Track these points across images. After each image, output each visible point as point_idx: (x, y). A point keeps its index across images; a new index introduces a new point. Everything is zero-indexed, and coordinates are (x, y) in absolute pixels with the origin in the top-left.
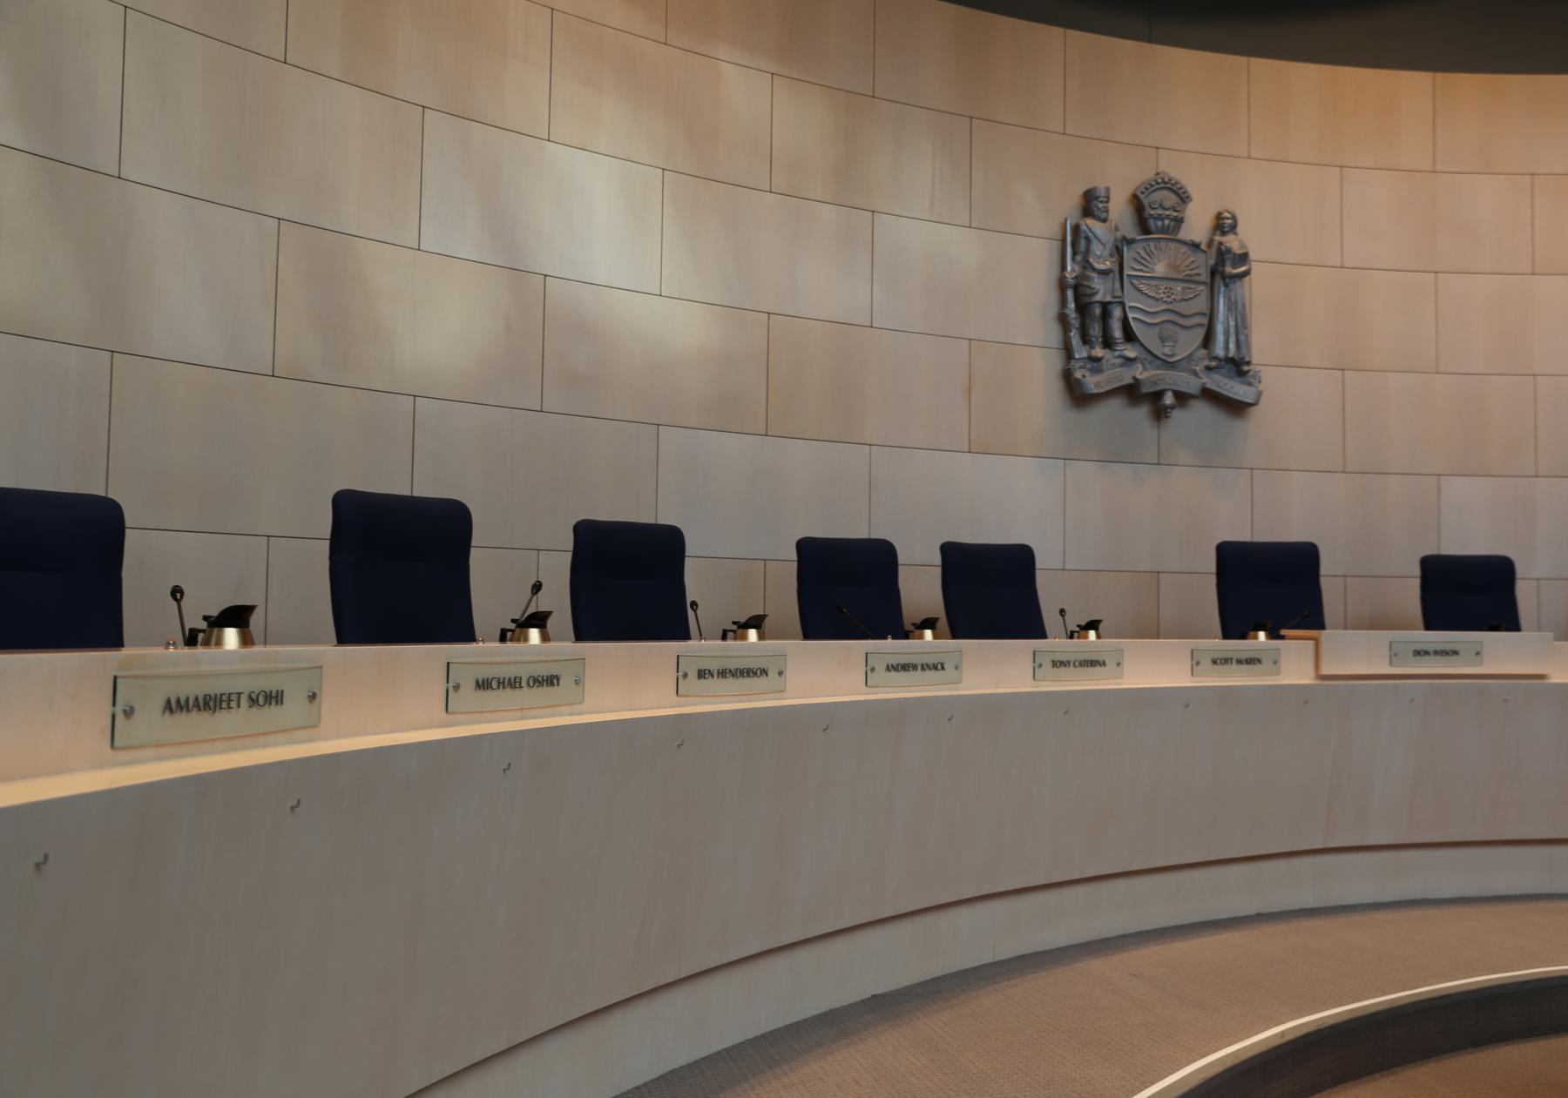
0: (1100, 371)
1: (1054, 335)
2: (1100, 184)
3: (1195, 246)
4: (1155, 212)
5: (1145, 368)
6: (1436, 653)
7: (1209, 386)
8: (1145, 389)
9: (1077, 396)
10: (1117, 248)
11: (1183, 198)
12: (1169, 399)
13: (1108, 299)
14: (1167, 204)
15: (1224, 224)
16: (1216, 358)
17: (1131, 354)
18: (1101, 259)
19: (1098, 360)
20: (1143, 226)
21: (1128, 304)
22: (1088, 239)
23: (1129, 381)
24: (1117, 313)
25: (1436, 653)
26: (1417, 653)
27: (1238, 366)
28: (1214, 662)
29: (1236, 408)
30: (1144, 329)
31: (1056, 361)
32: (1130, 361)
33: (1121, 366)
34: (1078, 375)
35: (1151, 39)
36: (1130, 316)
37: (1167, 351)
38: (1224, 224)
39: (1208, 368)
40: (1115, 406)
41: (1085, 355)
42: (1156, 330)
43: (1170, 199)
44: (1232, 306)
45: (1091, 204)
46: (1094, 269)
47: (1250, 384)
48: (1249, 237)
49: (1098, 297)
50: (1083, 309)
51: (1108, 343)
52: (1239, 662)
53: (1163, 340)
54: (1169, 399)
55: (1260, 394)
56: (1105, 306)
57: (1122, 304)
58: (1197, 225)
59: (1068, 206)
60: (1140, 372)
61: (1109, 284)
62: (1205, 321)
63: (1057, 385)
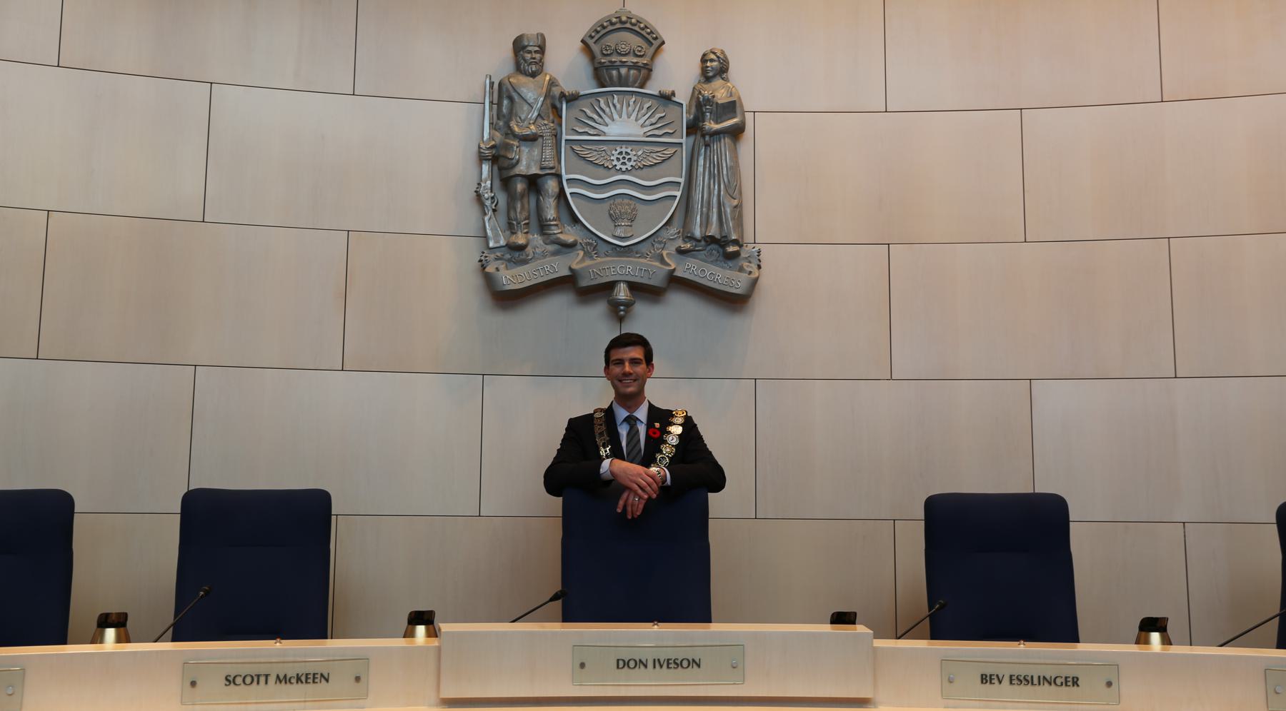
0: (525, 262)
2: (531, 30)
4: (620, 56)
5: (587, 254)
6: (658, 663)
7: (678, 273)
8: (584, 283)
10: (554, 107)
11: (654, 42)
12: (622, 293)
13: (534, 170)
14: (623, 48)
15: (714, 67)
16: (692, 238)
17: (570, 239)
18: (527, 121)
19: (521, 248)
20: (601, 74)
21: (565, 177)
22: (511, 99)
23: (566, 272)
24: (551, 185)
25: (658, 663)
26: (623, 664)
27: (724, 248)
28: (230, 681)
29: (734, 302)
32: (571, 246)
33: (555, 254)
34: (490, 269)
36: (568, 191)
37: (619, 232)
38: (714, 67)
39: (681, 252)
40: (558, 303)
41: (502, 242)
42: (606, 206)
43: (634, 41)
44: (715, 175)
45: (528, 55)
46: (515, 136)
47: (741, 269)
48: (748, 84)
49: (522, 169)
50: (506, 182)
51: (543, 227)
52: (283, 679)
53: (614, 218)
54: (622, 293)
55: (755, 282)
56: (534, 183)
57: (559, 176)
58: (676, 73)
60: (576, 261)
61: (536, 152)
62: (678, 194)
63: (476, 281)
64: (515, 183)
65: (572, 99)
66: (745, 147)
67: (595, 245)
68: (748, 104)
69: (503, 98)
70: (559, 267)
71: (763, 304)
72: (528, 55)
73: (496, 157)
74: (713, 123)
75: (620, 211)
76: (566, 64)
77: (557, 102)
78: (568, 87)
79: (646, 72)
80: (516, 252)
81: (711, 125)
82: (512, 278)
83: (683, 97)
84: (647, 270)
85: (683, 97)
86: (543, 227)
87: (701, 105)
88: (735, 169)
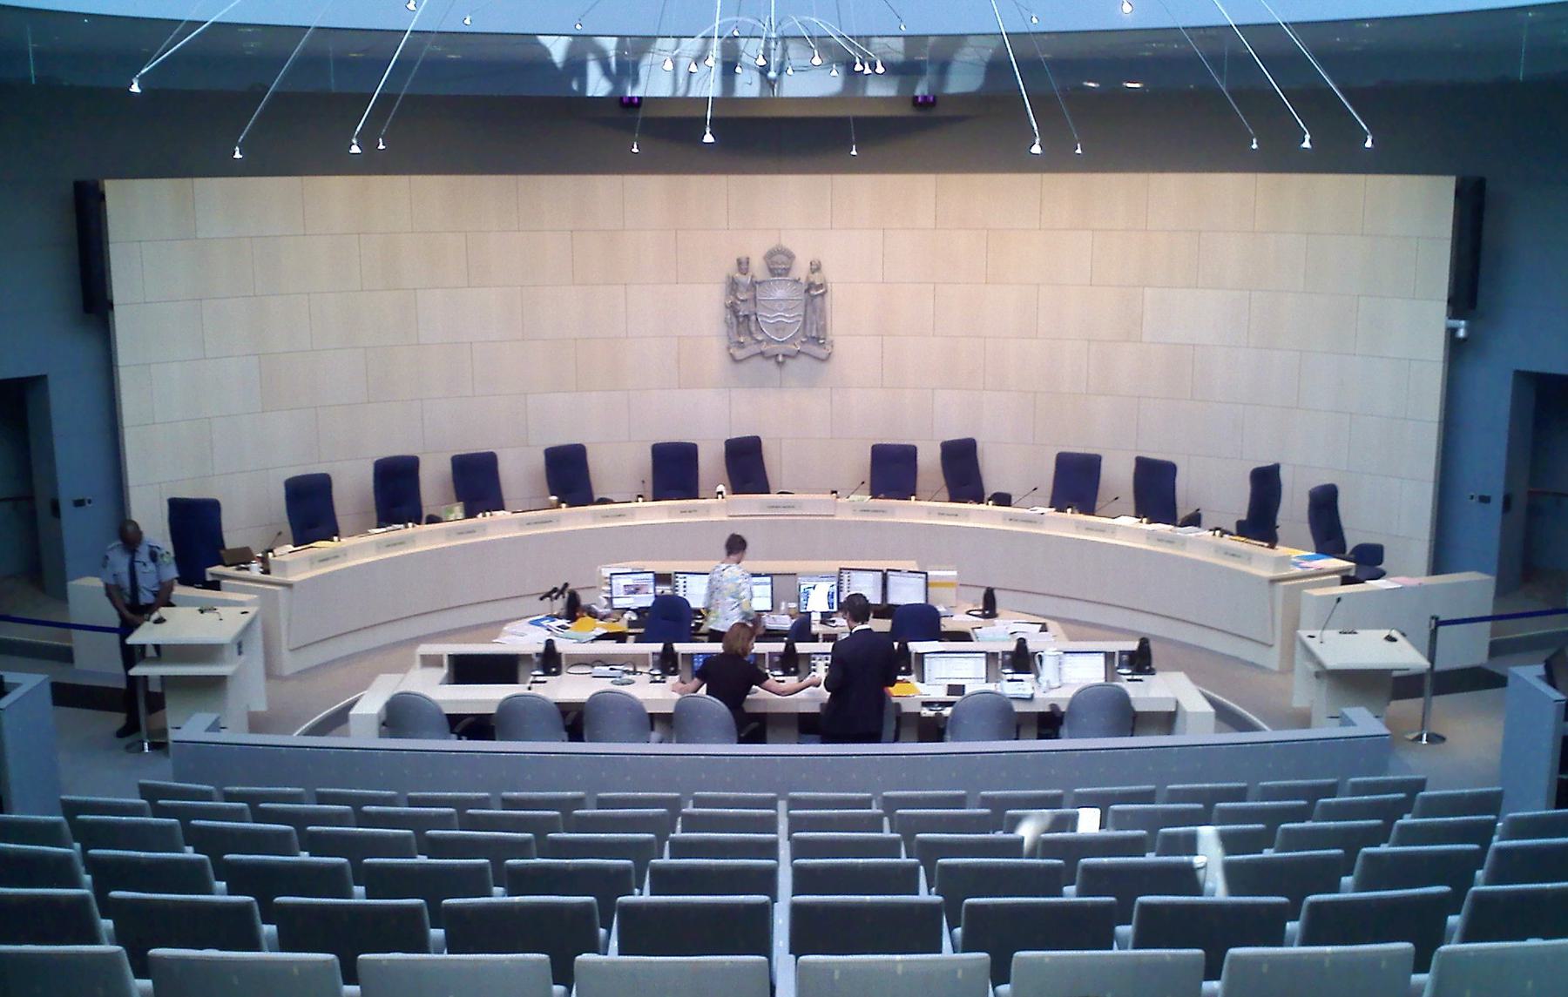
1: (723, 329)
2: (743, 255)
3: (797, 281)
4: (780, 264)
9: (735, 360)
15: (816, 268)
20: (772, 272)
30: (774, 321)
31: (725, 342)
35: (780, 172)
38: (816, 268)
40: (758, 361)
43: (784, 259)
44: (814, 311)
45: (743, 265)
48: (831, 274)
56: (747, 317)
58: (801, 270)
59: (730, 267)
60: (764, 347)
64: (741, 318)
65: (760, 283)
66: (828, 298)
67: (770, 340)
68: (829, 279)
69: (733, 285)
70: (756, 349)
71: (835, 360)
72: (743, 265)
73: (733, 308)
74: (814, 293)
75: (779, 327)
76: (758, 268)
77: (754, 284)
78: (759, 278)
79: (787, 271)
80: (741, 345)
81: (814, 292)
82: (739, 354)
83: (803, 280)
84: (793, 348)
85: (803, 280)
86: (751, 333)
87: (811, 286)
88: (823, 310)
